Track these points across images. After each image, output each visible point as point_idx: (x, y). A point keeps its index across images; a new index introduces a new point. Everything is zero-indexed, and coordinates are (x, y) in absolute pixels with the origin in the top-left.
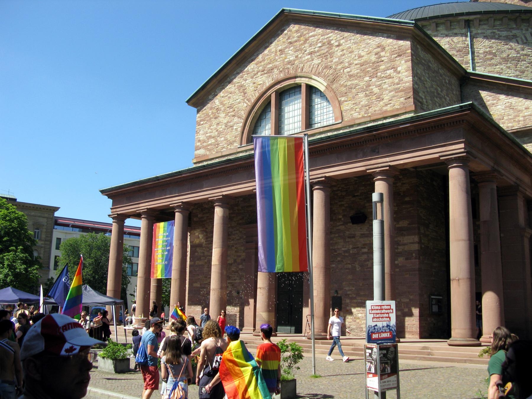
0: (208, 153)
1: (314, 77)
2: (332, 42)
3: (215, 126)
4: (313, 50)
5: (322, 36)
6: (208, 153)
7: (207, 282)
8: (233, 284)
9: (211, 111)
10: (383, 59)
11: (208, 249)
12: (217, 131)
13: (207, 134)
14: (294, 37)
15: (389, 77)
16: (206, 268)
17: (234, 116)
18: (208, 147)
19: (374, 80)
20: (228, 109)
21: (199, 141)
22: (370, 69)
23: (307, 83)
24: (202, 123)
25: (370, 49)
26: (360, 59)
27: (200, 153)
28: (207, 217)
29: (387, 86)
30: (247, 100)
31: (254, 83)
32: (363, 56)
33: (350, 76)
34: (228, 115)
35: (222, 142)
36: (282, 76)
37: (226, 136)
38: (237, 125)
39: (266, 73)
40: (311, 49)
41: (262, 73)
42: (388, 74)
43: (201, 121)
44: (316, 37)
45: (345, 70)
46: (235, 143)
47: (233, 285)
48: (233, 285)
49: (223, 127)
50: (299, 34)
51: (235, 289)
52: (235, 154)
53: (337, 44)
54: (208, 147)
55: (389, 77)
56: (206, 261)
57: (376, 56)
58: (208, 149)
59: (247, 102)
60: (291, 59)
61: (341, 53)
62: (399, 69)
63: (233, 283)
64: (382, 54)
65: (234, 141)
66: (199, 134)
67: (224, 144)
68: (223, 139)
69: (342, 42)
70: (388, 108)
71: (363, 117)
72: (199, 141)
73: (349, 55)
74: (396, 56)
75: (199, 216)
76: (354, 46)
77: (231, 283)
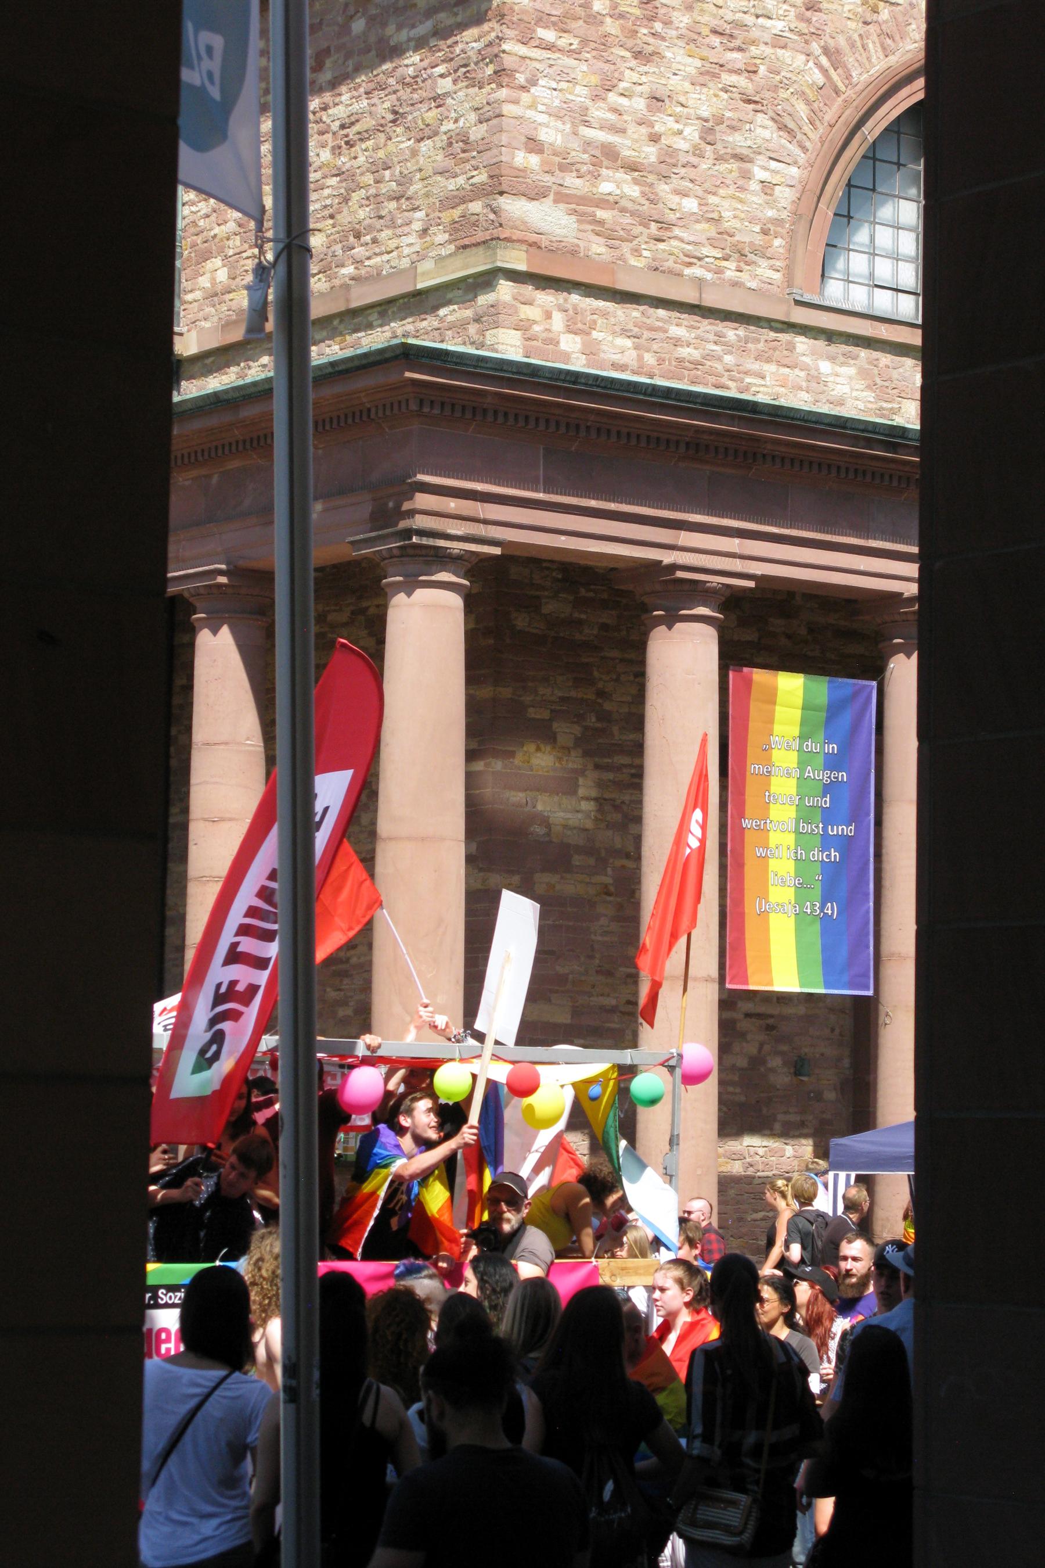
0: (598, 248)
3: (640, 104)
6: (598, 248)
7: (614, 1002)
8: (771, 1021)
11: (617, 817)
12: (655, 138)
13: (587, 123)
16: (603, 921)
17: (749, 102)
18: (601, 214)
20: (716, 40)
21: (533, 145)
24: (548, 35)
27: (544, 227)
28: (604, 627)
30: (826, 51)
34: (716, 76)
37: (712, 199)
38: (773, 164)
46: (764, 263)
47: (770, 1028)
48: (770, 1028)
49: (692, 132)
51: (785, 1048)
52: (772, 329)
54: (601, 214)
56: (608, 880)
58: (601, 223)
59: (824, 60)
63: (771, 1016)
65: (761, 252)
66: (525, 97)
67: (702, 239)
68: (690, 205)
75: (549, 607)
77: (759, 1016)
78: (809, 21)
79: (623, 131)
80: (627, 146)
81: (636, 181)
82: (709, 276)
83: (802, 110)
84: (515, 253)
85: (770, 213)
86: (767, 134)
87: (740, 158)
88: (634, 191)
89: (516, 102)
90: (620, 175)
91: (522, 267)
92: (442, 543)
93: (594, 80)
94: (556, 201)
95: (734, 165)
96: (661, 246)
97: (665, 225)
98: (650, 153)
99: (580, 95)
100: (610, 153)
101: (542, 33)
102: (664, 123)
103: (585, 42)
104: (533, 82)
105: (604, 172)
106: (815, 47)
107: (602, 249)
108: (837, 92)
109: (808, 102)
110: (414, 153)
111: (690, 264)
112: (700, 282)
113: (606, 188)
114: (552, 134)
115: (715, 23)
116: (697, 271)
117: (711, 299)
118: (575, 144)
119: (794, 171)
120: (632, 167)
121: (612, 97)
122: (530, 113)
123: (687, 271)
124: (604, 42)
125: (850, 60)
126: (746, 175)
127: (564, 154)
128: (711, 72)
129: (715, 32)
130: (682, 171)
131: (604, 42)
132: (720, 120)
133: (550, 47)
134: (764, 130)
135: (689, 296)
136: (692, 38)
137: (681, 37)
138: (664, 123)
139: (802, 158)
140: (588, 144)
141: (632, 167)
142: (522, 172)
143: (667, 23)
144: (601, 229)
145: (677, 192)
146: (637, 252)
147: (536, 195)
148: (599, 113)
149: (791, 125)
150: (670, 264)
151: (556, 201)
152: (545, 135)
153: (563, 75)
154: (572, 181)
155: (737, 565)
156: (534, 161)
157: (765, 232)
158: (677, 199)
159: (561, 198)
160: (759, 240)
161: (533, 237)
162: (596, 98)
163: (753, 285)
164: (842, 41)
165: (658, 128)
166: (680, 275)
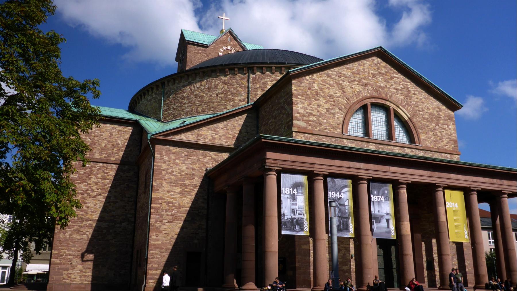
0: (310, 128)
1: (400, 107)
2: (410, 89)
3: (316, 107)
4: (397, 87)
5: (403, 81)
6: (310, 128)
9: (309, 91)
10: (441, 117)
12: (318, 111)
13: (307, 110)
14: (382, 70)
15: (445, 129)
18: (310, 123)
19: (437, 127)
20: (328, 97)
21: (298, 113)
22: (435, 119)
23: (395, 108)
24: (300, 97)
25: (434, 107)
26: (429, 110)
27: (300, 124)
29: (445, 134)
30: (347, 98)
31: (352, 88)
32: (430, 109)
33: (424, 118)
34: (328, 102)
35: (324, 123)
36: (375, 94)
37: (328, 120)
39: (361, 85)
40: (396, 86)
41: (358, 83)
42: (444, 127)
43: (299, 95)
44: (399, 79)
45: (420, 113)
49: (325, 110)
50: (386, 70)
53: (413, 92)
54: (310, 123)
55: (445, 129)
57: (437, 113)
58: (310, 124)
59: (346, 100)
60: (382, 85)
61: (416, 100)
62: (450, 127)
64: (441, 113)
65: (338, 128)
68: (325, 121)
69: (416, 93)
70: (446, 147)
71: (433, 148)
72: (298, 113)
73: (422, 104)
74: (448, 118)
76: (424, 100)
78: (343, 94)
79: (313, 111)
80: (314, 113)
81: (315, 118)
82: (329, 131)
83: (343, 107)
84: (295, 129)
85: (338, 122)
86: (338, 110)
87: (333, 114)
88: (315, 119)
89: (295, 107)
90: (313, 117)
91: (297, 131)
92: (271, 167)
93: (308, 103)
94: (302, 121)
95: (332, 115)
96: (321, 127)
97: (321, 124)
98: (318, 113)
99: (306, 105)
100: (311, 114)
101: (299, 97)
102: (320, 109)
103: (306, 98)
104: (298, 104)
105: (310, 116)
106: (345, 98)
107: (311, 128)
108: (349, 104)
109: (344, 106)
110: (283, 117)
111: (325, 130)
112: (327, 132)
113: (311, 119)
114: (301, 111)
115: (328, 95)
116: (327, 131)
117: (329, 135)
118: (305, 113)
119: (342, 116)
120: (315, 116)
121: (311, 106)
122: (297, 108)
123: (325, 131)
124: (310, 98)
125: (351, 99)
126: (335, 117)
127: (303, 114)
128: (327, 102)
129: (328, 96)
130: (323, 116)
131: (310, 98)
132: (329, 108)
133: (300, 99)
134: (337, 110)
135: (326, 134)
136: (324, 97)
137: (322, 97)
138: (320, 109)
139: (344, 114)
140: (307, 113)
141: (315, 116)
142: (297, 117)
143: (320, 95)
144: (310, 125)
145: (322, 119)
146: (316, 128)
147: (299, 120)
148: (309, 108)
149: (341, 109)
150: (322, 130)
151: (302, 121)
152: (300, 111)
153: (302, 103)
154: (305, 118)
155: (326, 170)
156: (298, 115)
157: (338, 125)
158: (323, 120)
159: (303, 120)
160: (337, 126)
161: (298, 126)
162: (308, 106)
163: (336, 132)
164: (349, 97)
165: (319, 110)
166: (324, 131)
